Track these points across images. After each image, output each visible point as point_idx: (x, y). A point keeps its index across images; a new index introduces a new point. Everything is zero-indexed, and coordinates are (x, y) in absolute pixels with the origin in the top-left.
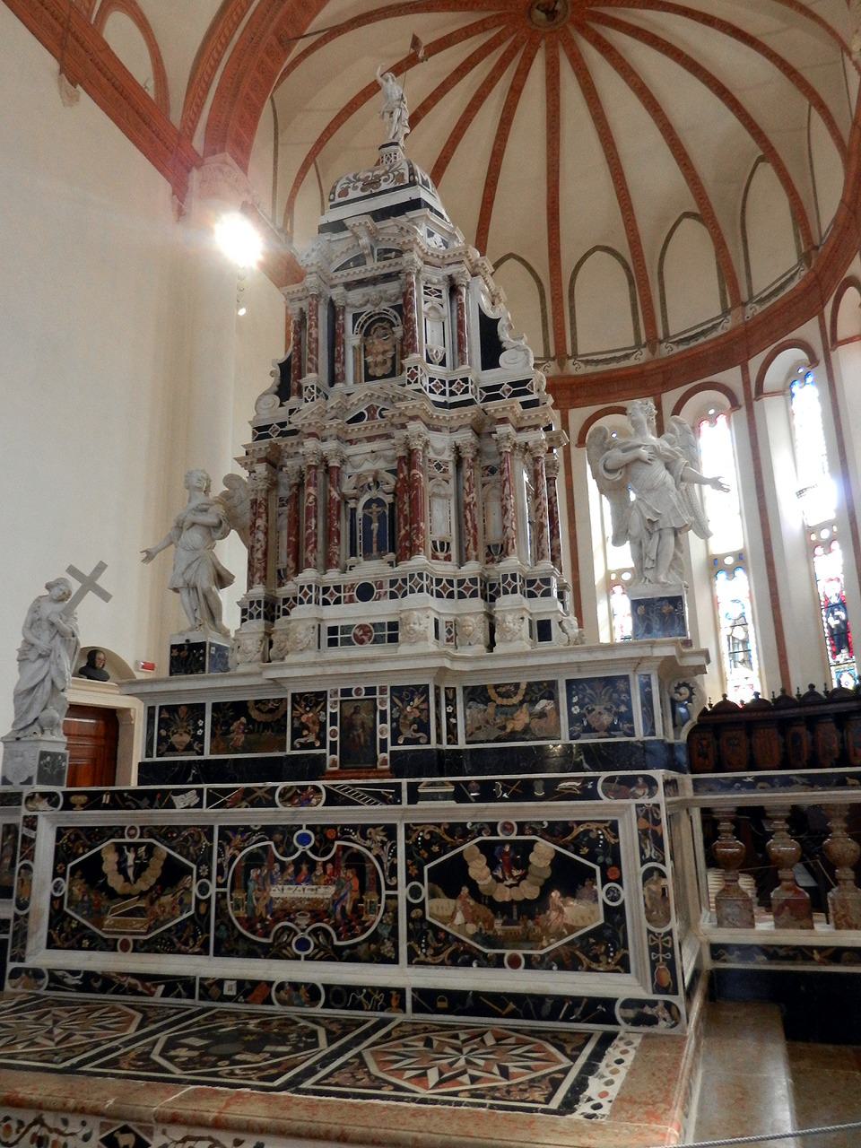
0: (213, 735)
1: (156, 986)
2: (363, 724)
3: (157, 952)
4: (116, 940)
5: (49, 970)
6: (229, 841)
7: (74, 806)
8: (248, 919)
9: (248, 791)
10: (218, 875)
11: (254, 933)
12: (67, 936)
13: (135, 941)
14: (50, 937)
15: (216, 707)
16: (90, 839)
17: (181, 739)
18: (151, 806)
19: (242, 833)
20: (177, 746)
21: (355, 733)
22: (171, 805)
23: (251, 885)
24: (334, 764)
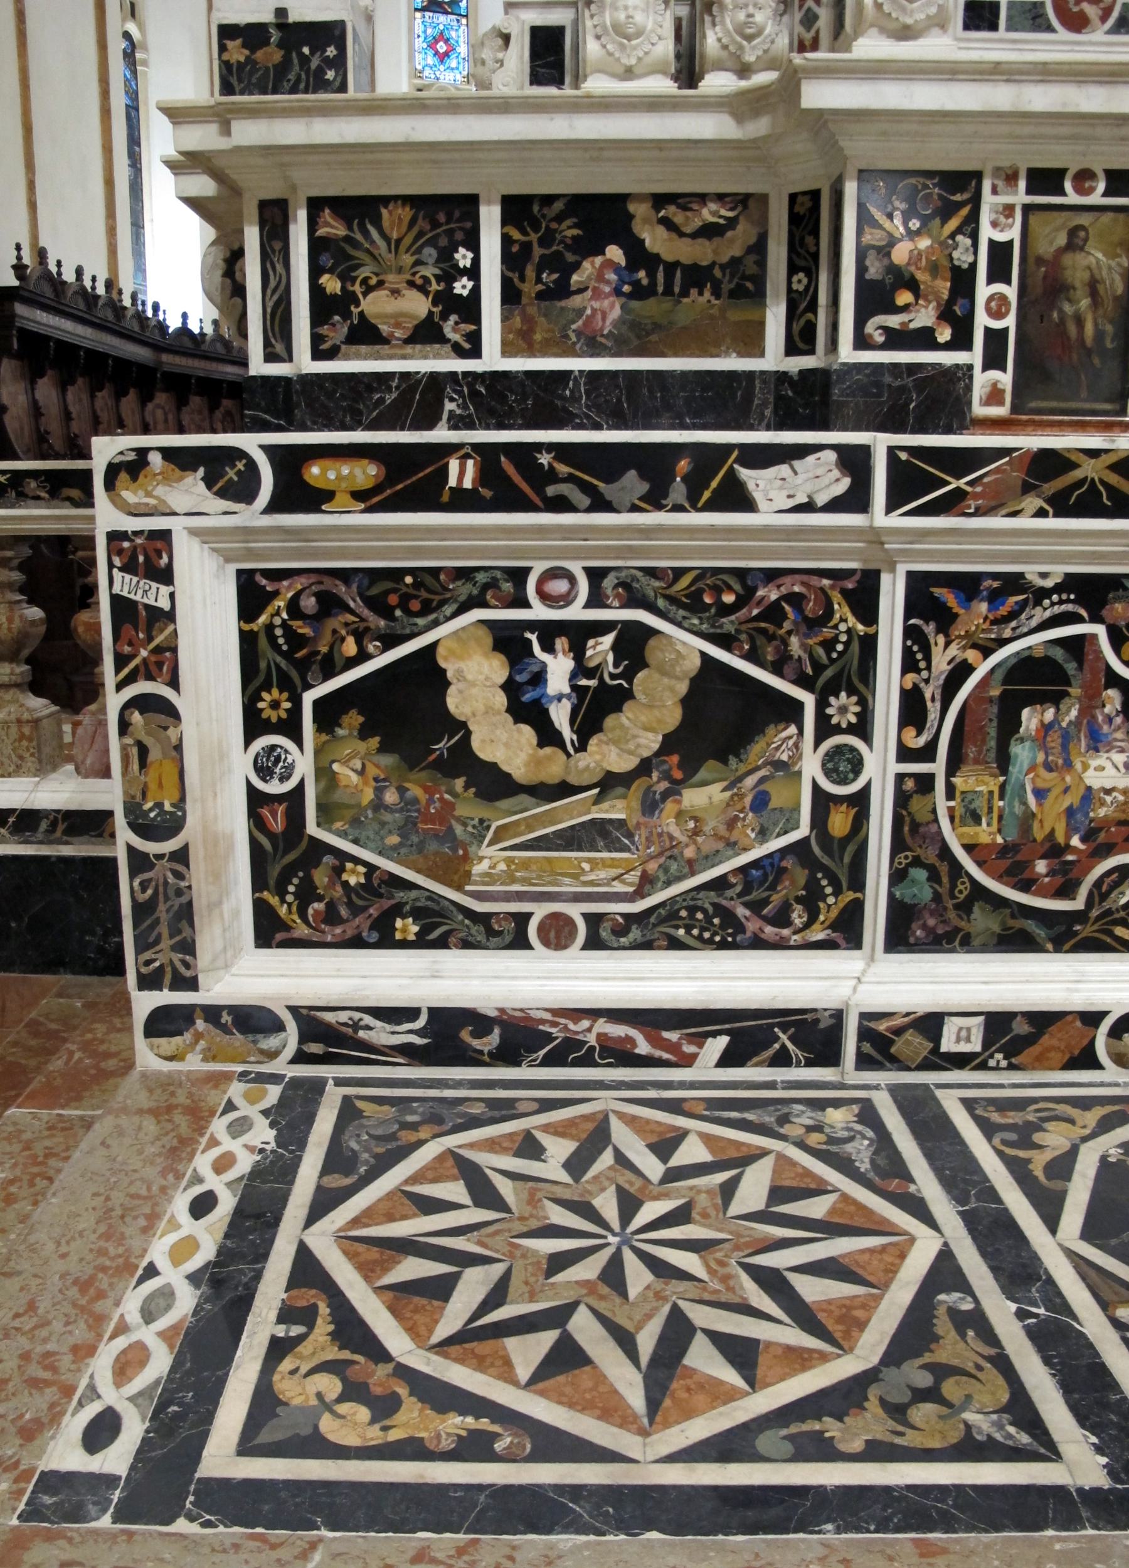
0: (510, 295)
1: (700, 1039)
2: (1093, 287)
3: (675, 944)
4: (522, 919)
5: (294, 1010)
6: (945, 620)
7: (328, 495)
8: (1006, 850)
9: (1048, 464)
10: (903, 724)
11: (1025, 886)
12: (331, 906)
13: (594, 920)
14: (262, 911)
15: (516, 209)
16: (386, 612)
17: (398, 305)
18: (655, 500)
19: (994, 597)
20: (384, 329)
21: (1068, 308)
22: (737, 498)
23: (1022, 753)
24: (994, 396)
